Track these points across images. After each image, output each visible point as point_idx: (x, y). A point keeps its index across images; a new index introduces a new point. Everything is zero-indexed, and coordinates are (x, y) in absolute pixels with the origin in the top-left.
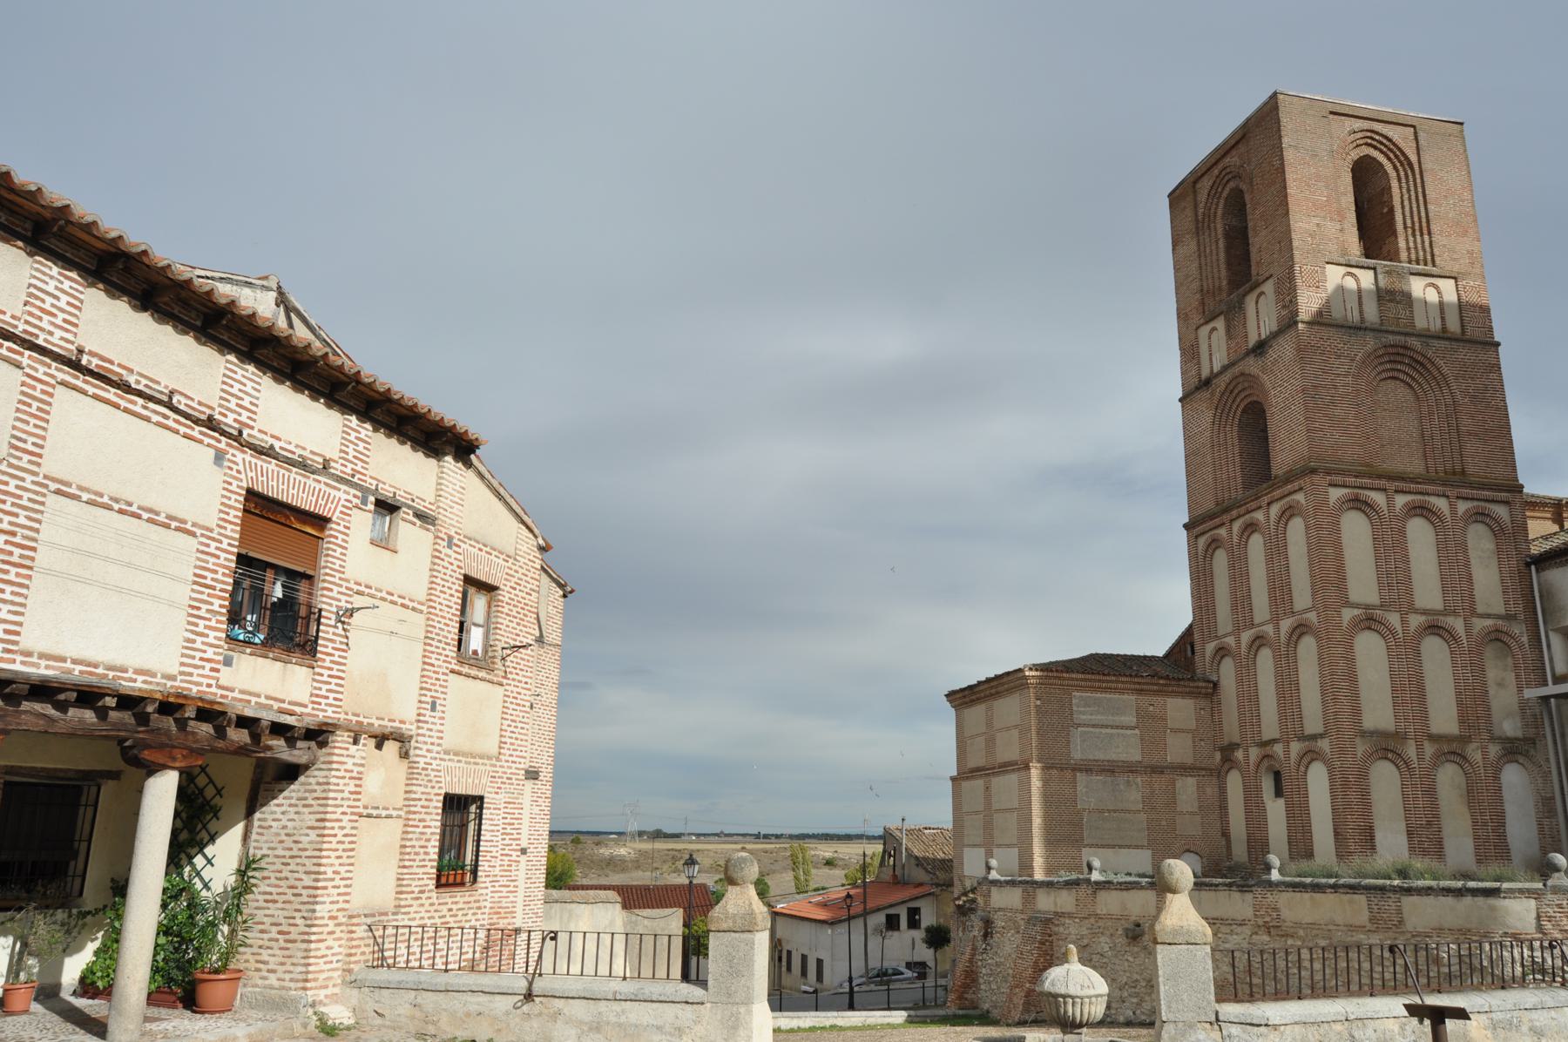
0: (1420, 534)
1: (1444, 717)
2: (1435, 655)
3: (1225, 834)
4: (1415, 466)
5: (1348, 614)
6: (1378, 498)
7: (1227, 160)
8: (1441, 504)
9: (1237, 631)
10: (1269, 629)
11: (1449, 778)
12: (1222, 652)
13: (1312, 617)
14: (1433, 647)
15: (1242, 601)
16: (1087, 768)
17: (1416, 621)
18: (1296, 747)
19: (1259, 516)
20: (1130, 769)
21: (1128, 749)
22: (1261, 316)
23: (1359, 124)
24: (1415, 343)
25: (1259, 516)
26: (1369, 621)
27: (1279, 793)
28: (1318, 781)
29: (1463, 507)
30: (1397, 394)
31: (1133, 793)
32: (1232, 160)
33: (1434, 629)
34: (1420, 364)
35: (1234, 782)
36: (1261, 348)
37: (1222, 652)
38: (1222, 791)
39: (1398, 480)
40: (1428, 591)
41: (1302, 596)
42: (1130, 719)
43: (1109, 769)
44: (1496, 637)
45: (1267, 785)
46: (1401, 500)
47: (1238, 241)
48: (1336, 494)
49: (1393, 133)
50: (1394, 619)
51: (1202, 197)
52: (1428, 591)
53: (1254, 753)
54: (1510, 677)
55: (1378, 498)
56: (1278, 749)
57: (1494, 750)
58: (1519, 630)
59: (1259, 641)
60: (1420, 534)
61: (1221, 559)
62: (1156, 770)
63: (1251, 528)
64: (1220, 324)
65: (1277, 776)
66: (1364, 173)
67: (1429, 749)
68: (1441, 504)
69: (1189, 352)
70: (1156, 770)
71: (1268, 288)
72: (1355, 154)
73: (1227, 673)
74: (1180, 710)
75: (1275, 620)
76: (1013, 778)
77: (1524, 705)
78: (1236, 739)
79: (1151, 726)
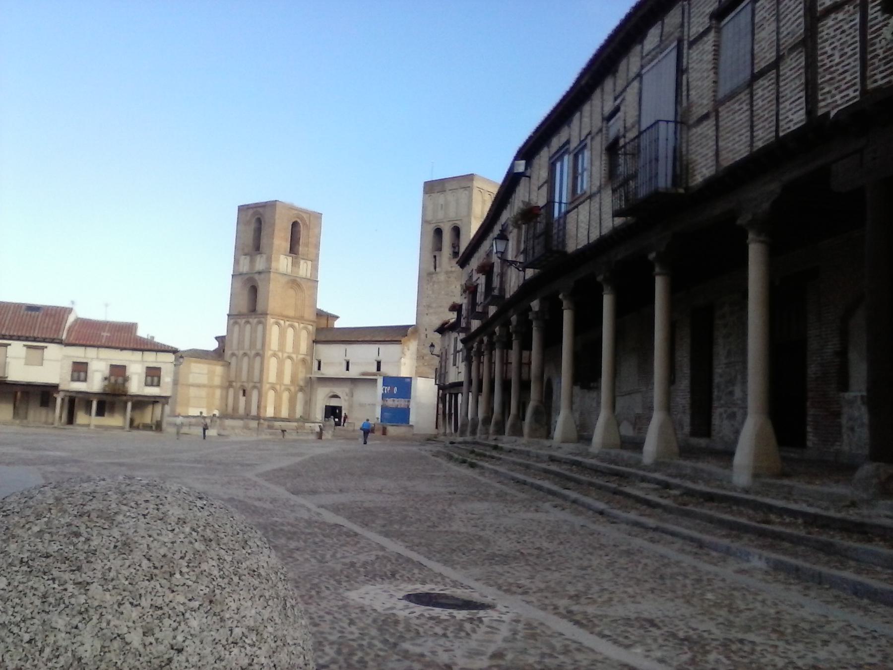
0: (290, 332)
1: (287, 380)
2: (288, 363)
3: (226, 405)
4: (291, 313)
6: (282, 322)
7: (258, 209)
8: (296, 324)
9: (238, 350)
11: (285, 396)
12: (233, 355)
14: (289, 362)
16: (193, 385)
17: (286, 355)
18: (251, 384)
19: (251, 320)
20: (204, 386)
21: (204, 380)
22: (260, 264)
23: (296, 212)
24: (298, 280)
25: (251, 320)
26: (275, 355)
27: (244, 395)
28: (255, 394)
29: (302, 325)
30: (291, 292)
31: (203, 392)
32: (261, 210)
33: (289, 357)
34: (299, 285)
35: (231, 391)
36: (260, 273)
38: (227, 392)
39: (286, 318)
40: (289, 347)
42: (206, 371)
43: (199, 386)
44: (304, 361)
45: (241, 393)
46: (287, 323)
47: (258, 231)
48: (272, 321)
49: (305, 216)
50: (280, 354)
52: (289, 347)
53: (239, 384)
54: (304, 370)
55: (282, 322)
56: (245, 384)
57: (297, 388)
58: (308, 358)
60: (290, 332)
62: (211, 387)
63: (248, 322)
64: (248, 258)
65: (244, 391)
66: (295, 225)
67: (283, 387)
68: (296, 324)
69: (237, 262)
70: (211, 387)
71: (264, 256)
72: (294, 220)
73: (233, 361)
75: (250, 349)
77: (306, 378)
78: (234, 379)
79: (211, 374)
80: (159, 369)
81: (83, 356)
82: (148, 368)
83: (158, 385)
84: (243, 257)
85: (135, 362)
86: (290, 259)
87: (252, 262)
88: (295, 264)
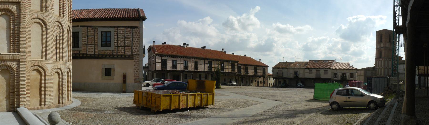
5: (385, 67)
10: (380, 68)
12: (377, 68)
13: (383, 67)
14: (390, 69)
15: (379, 65)
19: (380, 60)
25: (380, 60)
26: (386, 68)
33: (390, 68)
37: (377, 68)
41: (383, 66)
46: (389, 60)
50: (388, 68)
51: (379, 33)
59: (380, 68)
61: (377, 62)
63: (380, 60)
66: (390, 35)
73: (377, 70)
74: (374, 72)
75: (381, 67)
76: (358, 75)
80: (353, 74)
81: (336, 71)
82: (350, 74)
83: (353, 78)
84: (378, 44)
85: (348, 72)
86: (389, 44)
87: (380, 45)
88: (390, 45)
